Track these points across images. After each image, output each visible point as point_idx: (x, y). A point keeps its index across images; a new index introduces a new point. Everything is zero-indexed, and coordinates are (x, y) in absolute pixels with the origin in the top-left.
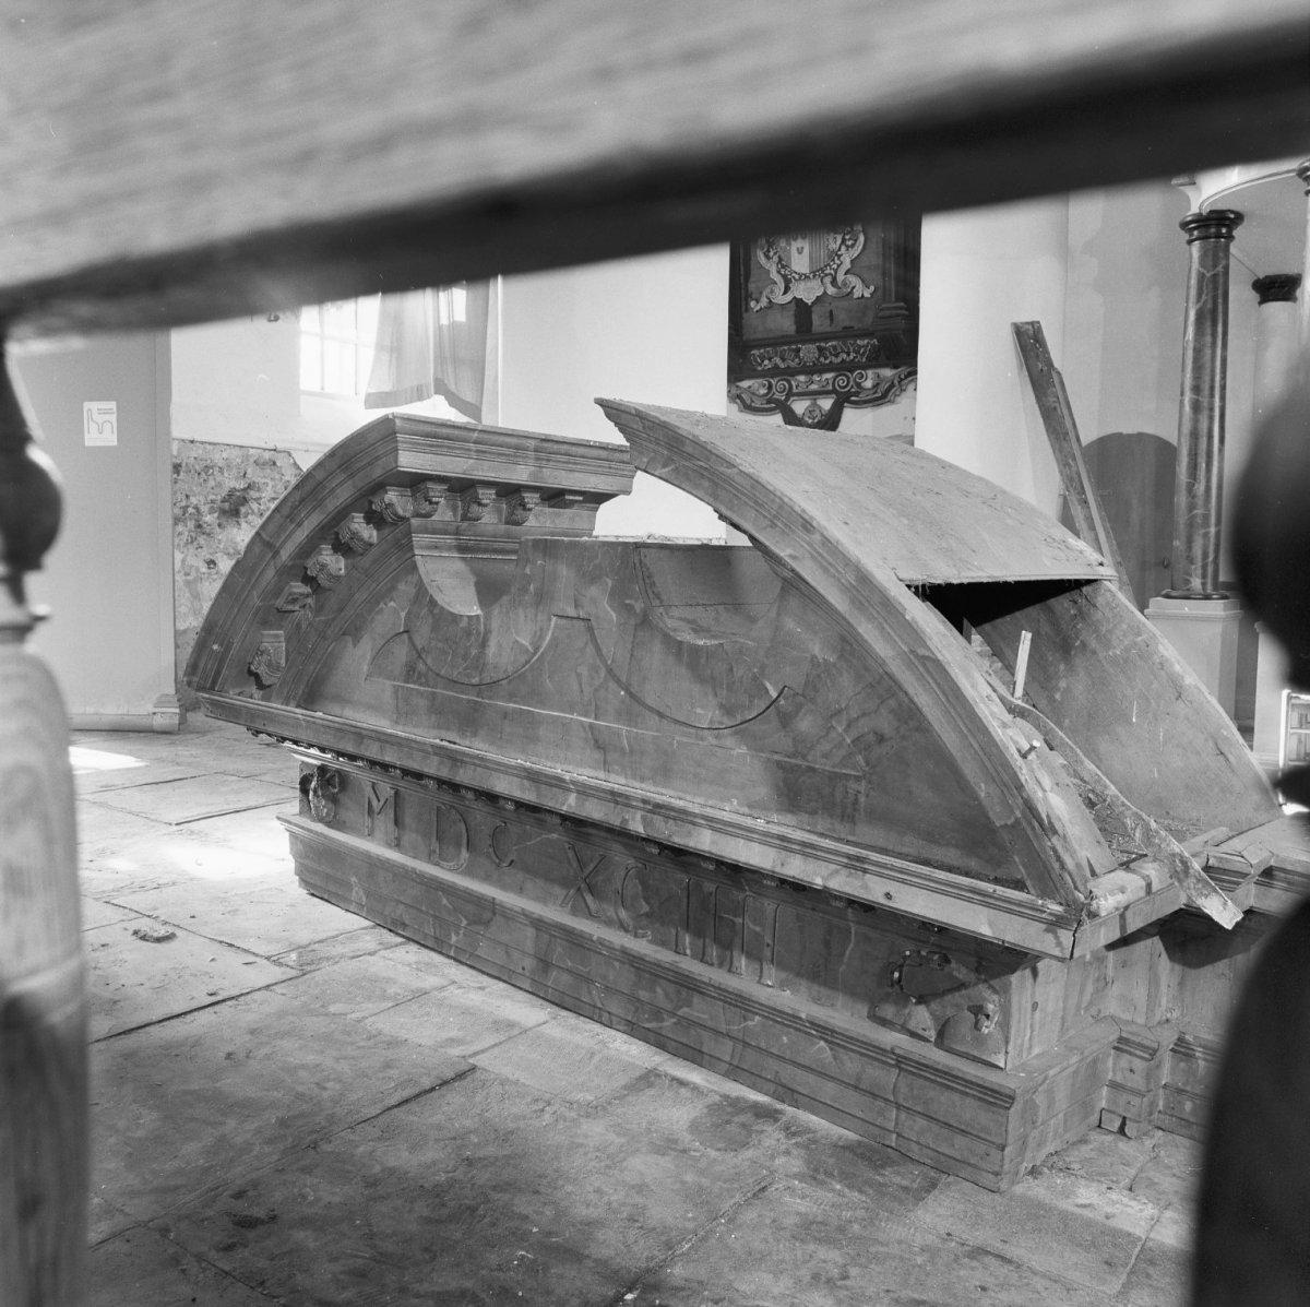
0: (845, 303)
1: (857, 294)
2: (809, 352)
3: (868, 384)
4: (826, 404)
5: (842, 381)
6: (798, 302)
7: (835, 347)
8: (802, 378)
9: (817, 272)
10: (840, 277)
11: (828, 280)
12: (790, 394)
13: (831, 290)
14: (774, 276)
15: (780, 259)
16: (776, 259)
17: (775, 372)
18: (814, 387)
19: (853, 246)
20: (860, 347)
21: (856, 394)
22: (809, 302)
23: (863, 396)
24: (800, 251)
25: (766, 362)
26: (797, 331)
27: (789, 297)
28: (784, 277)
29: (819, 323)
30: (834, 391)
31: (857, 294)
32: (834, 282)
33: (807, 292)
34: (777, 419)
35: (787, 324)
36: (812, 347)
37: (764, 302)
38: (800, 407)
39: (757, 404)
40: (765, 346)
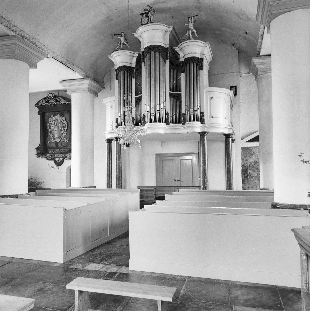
0: (64, 142)
1: (66, 141)
2: (58, 150)
3: (68, 156)
4: (61, 159)
5: (63, 155)
6: (56, 142)
7: (62, 150)
8: (57, 154)
9: (59, 137)
10: (63, 138)
11: (61, 138)
12: (55, 157)
13: (61, 140)
14: (52, 137)
15: (53, 135)
16: (52, 134)
17: (52, 153)
18: (59, 156)
19: (65, 133)
20: (66, 150)
21: (66, 158)
22: (58, 142)
23: (67, 158)
24: (56, 133)
25: (51, 152)
26: (56, 147)
27: (54, 141)
28: (53, 137)
29: (59, 145)
30: (62, 157)
31: (66, 141)
32: (62, 139)
33: (57, 140)
34: (52, 162)
35: (54, 145)
36: (59, 150)
37: (50, 141)
38: (57, 159)
39: (49, 159)
40: (50, 149)
